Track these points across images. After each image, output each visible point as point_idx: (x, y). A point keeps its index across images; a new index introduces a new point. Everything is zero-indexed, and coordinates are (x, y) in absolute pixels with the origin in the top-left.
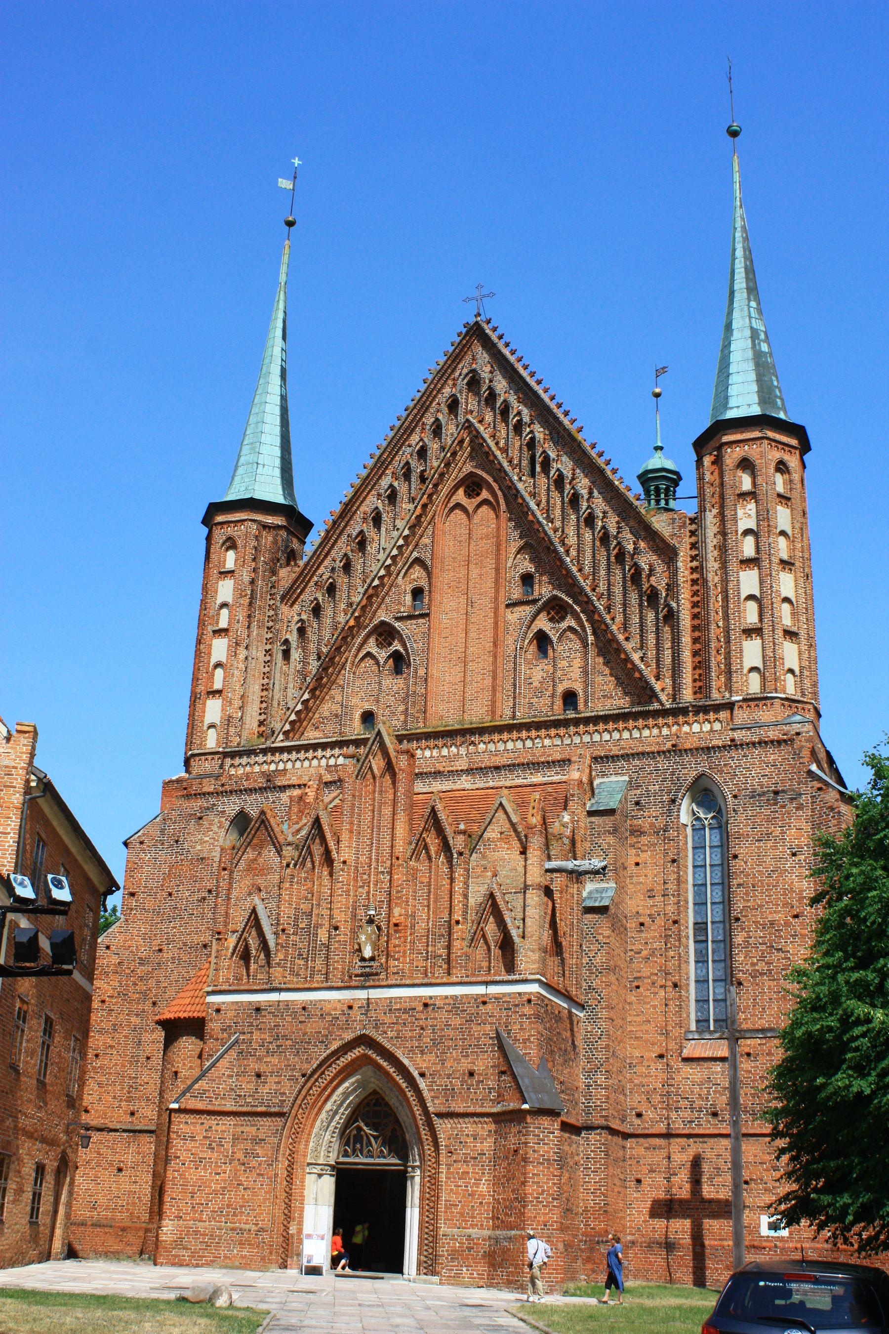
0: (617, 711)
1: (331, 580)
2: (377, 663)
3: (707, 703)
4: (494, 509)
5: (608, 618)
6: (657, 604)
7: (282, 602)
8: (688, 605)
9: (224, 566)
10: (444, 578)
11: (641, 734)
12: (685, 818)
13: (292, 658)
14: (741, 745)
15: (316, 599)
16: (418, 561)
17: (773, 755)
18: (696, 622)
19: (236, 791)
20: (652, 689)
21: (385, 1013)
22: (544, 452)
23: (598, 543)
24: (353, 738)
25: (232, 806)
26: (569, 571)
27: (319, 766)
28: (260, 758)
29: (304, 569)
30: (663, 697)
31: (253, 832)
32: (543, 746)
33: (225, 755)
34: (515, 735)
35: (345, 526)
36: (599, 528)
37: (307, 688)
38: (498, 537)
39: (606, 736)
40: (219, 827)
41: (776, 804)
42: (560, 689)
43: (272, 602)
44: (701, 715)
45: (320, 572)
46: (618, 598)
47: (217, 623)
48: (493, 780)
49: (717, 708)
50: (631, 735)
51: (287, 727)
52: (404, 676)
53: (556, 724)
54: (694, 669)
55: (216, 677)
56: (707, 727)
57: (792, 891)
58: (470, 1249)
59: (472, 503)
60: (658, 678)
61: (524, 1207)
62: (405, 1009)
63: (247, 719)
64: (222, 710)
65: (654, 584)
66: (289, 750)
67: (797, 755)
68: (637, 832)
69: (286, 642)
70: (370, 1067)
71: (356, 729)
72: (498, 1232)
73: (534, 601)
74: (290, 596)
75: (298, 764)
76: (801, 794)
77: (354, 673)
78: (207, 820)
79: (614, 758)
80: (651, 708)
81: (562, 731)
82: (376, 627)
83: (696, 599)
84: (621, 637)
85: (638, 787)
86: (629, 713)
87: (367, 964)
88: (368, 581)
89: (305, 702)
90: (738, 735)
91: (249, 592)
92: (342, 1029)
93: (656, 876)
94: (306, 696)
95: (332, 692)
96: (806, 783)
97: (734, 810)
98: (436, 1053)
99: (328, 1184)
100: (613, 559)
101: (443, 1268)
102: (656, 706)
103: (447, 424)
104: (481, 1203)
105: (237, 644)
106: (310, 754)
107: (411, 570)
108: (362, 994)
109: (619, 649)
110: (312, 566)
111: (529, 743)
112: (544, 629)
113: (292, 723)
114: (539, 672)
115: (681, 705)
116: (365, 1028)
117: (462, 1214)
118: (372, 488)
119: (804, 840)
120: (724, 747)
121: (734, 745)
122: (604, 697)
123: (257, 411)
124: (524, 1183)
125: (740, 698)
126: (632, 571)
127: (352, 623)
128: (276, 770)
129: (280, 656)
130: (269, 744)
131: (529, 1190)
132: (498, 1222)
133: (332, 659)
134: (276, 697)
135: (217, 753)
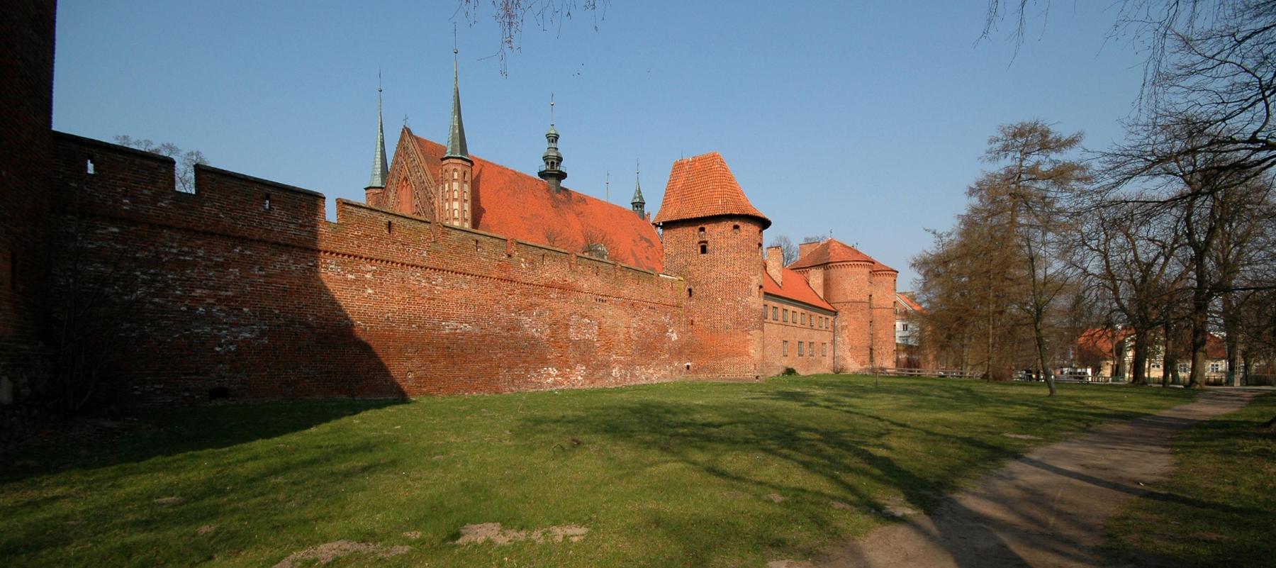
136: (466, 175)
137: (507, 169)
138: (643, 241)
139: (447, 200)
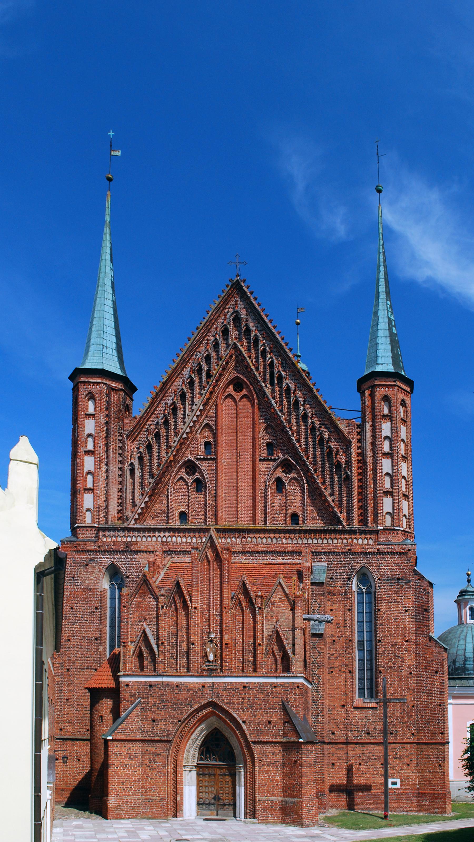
0: (321, 528)
1: (157, 430)
2: (187, 484)
3: (366, 529)
4: (250, 401)
5: (315, 475)
6: (341, 471)
7: (127, 439)
8: (356, 474)
9: (87, 411)
10: (223, 439)
11: (333, 542)
12: (354, 588)
13: (136, 476)
14: (382, 553)
15: (148, 440)
16: (207, 426)
17: (397, 560)
18: (360, 484)
19: (108, 551)
20: (338, 518)
21: (223, 690)
22: (279, 371)
23: (309, 432)
24: (177, 527)
25: (106, 560)
26: (294, 446)
27: (157, 541)
28: (121, 533)
29: (140, 421)
30: (345, 524)
31: (139, 586)
32: (282, 543)
33: (99, 529)
34: (267, 535)
35: (163, 397)
36: (310, 423)
37: (147, 494)
38: (254, 418)
39: (315, 541)
40: (99, 572)
41: (398, 585)
43: (120, 438)
44: (363, 535)
45: (149, 423)
46: (319, 464)
47: (86, 446)
48: (256, 558)
49: (371, 532)
50: (328, 542)
51: (137, 516)
52: (203, 493)
54: (359, 509)
55: (88, 480)
56: (365, 542)
57: (405, 629)
58: (272, 806)
59: (238, 395)
60: (341, 513)
61: (302, 788)
62: (233, 689)
63: (110, 508)
64: (94, 501)
65: (339, 460)
66: (139, 530)
67: (409, 561)
68: (331, 593)
69: (132, 464)
70: (215, 717)
72: (287, 799)
73: (275, 460)
74: (132, 436)
75: (144, 539)
76: (410, 581)
77: (174, 488)
78: (91, 567)
80: (338, 528)
81: (292, 536)
82: (185, 463)
83: (361, 471)
84: (322, 487)
85: (331, 570)
86: (328, 530)
87: (211, 664)
88: (180, 434)
89: (146, 503)
90: (380, 547)
91: (105, 429)
92: (200, 697)
93: (341, 617)
94: (147, 499)
95: (161, 498)
96: (413, 576)
97: (379, 586)
98: (251, 712)
99: (194, 773)
100: (317, 442)
101: (259, 816)
102: (340, 528)
103: (222, 343)
104: (277, 785)
105: (101, 461)
106: (151, 534)
107: (204, 431)
109: (321, 494)
110: (144, 419)
111: (274, 541)
112: (281, 477)
113: (139, 514)
114: (278, 500)
115: (353, 529)
116: (212, 697)
117: (267, 790)
118: (178, 375)
119: (411, 604)
120: (374, 553)
121: (379, 552)
122: (313, 518)
123: (99, 309)
124: (301, 777)
125: (382, 528)
126: (328, 450)
128: (131, 541)
129: (128, 472)
130: (125, 525)
131: (303, 780)
132: (286, 793)
133: (161, 479)
134: (128, 497)
135: (95, 527)
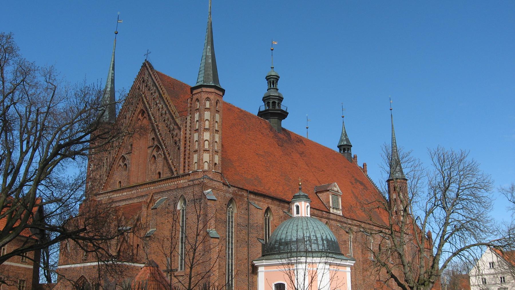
42: (157, 172)
53: (158, 181)
71: (118, 187)
79: (165, 191)
108: (82, 265)
127: (115, 156)
136: (218, 104)
137: (234, 106)
138: (358, 183)
139: (197, 130)
